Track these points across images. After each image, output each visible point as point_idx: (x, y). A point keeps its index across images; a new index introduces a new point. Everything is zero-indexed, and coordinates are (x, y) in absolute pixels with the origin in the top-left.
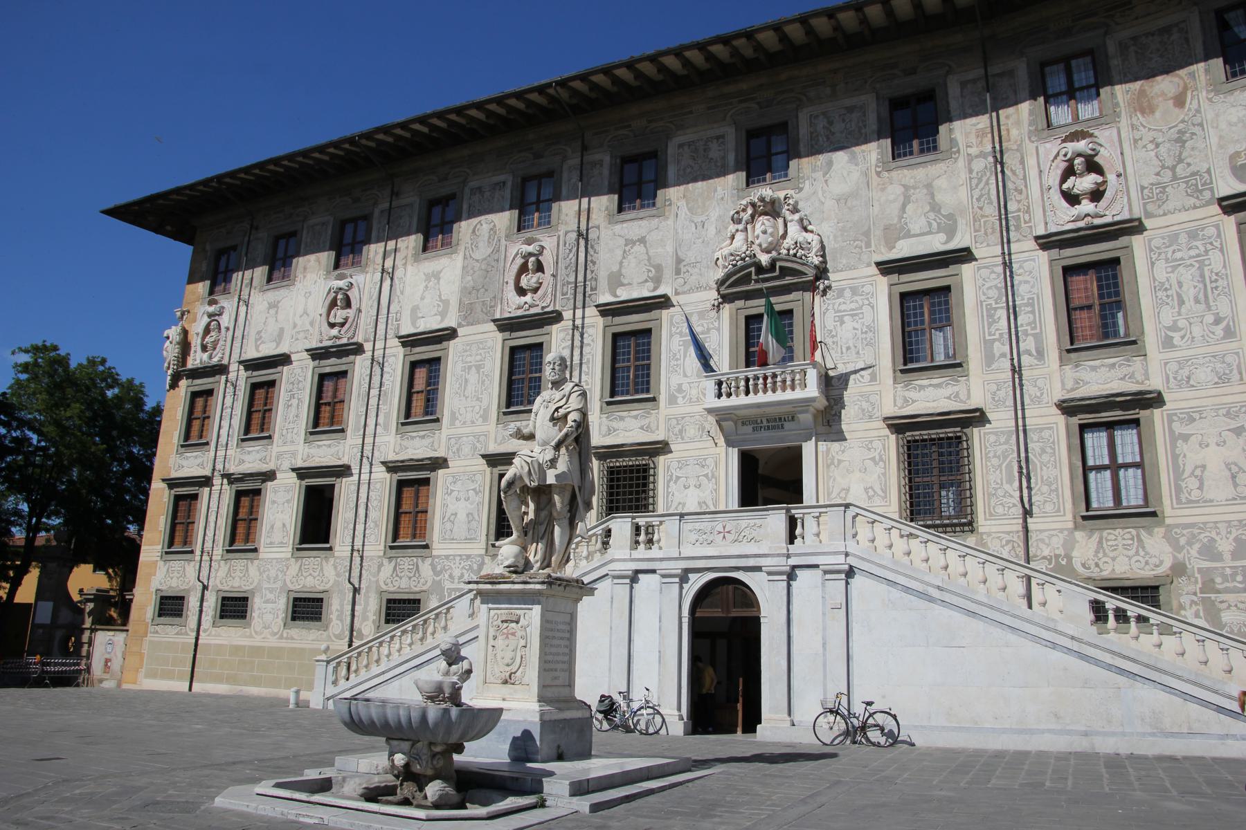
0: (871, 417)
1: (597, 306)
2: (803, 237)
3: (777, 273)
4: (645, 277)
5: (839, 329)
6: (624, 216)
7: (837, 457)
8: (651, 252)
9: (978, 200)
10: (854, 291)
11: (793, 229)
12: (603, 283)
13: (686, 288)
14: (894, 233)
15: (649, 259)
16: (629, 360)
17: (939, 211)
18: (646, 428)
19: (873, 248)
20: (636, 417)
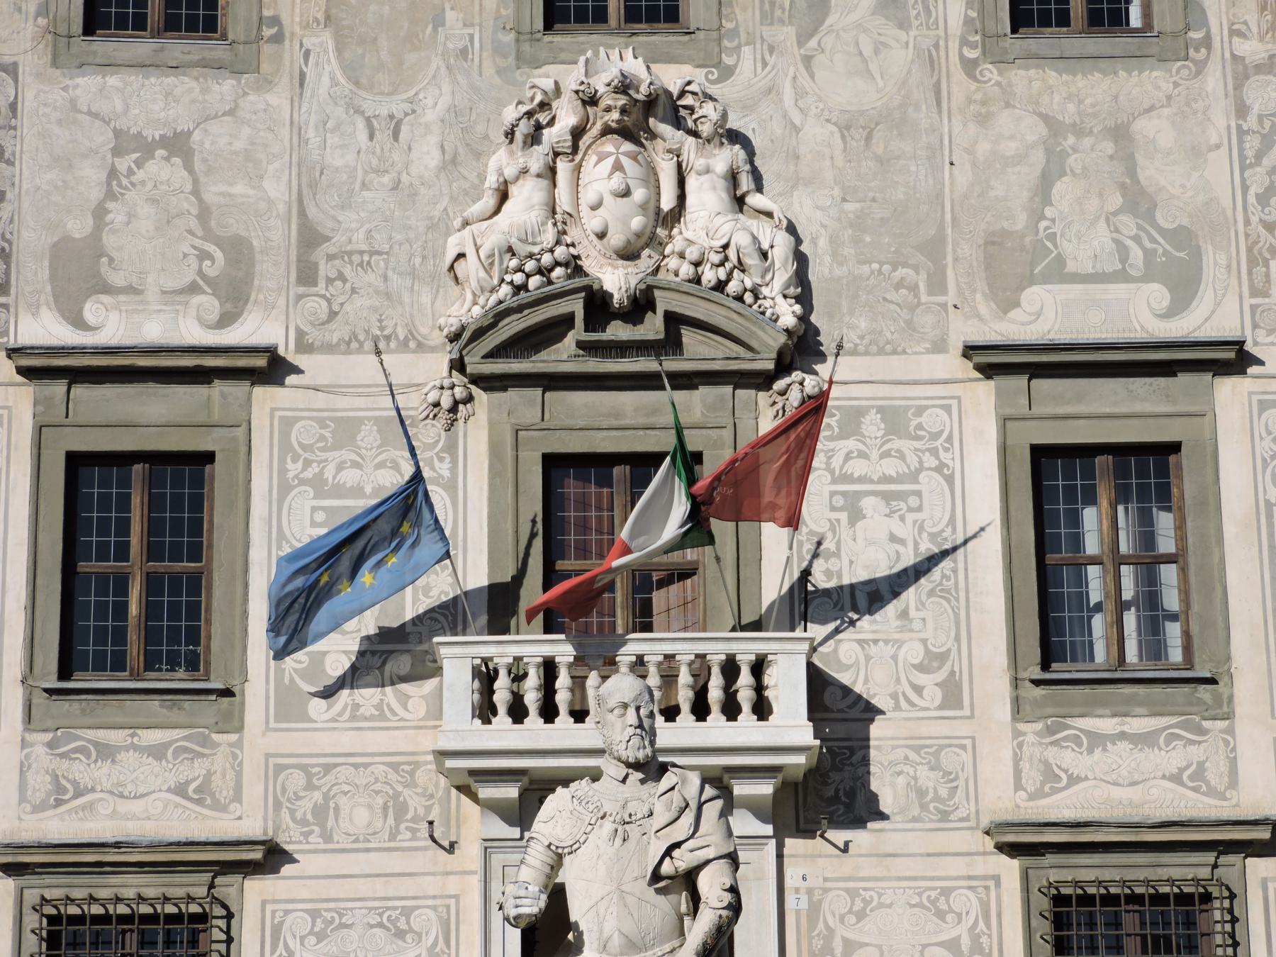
0: (944, 816)
1: (12, 352)
2: (740, 233)
3: (652, 328)
4: (190, 276)
5: (845, 533)
6: (104, 46)
7: (840, 932)
8: (211, 194)
9: (1263, 199)
10: (895, 421)
11: (706, 198)
12: (32, 272)
13: (336, 333)
14: (1018, 261)
15: (204, 213)
16: (123, 552)
17: (1150, 216)
18: (201, 794)
19: (951, 298)
20: (158, 752)
